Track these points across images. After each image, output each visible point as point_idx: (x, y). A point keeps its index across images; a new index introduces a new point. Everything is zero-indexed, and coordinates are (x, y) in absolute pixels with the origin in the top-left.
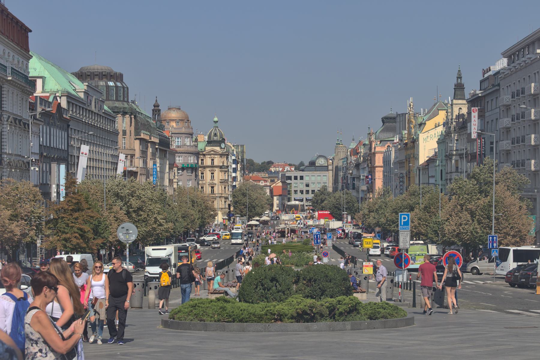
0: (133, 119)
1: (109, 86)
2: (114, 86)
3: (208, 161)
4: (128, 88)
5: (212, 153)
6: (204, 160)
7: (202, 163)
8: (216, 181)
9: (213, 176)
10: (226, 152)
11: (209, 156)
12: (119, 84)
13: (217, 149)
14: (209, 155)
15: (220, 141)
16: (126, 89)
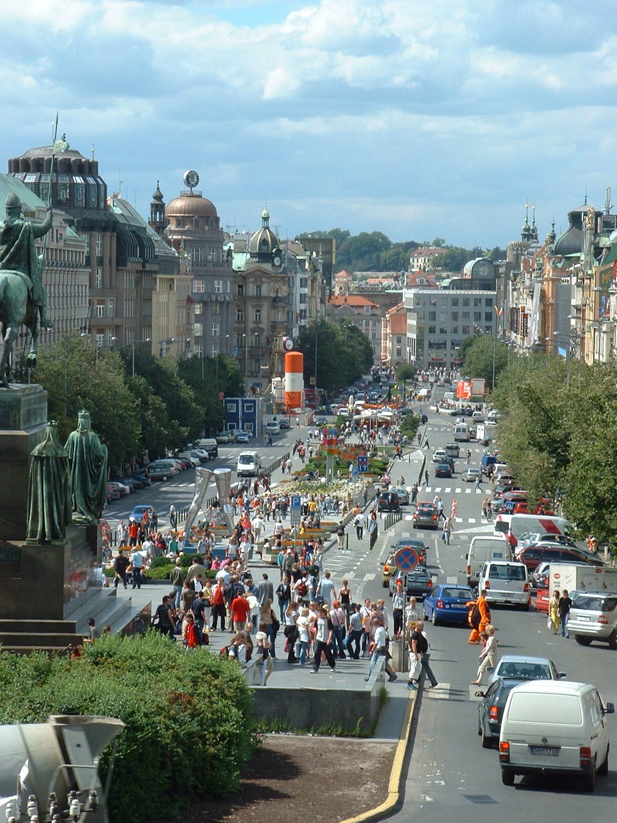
0: (115, 239)
1: (74, 183)
2: (82, 184)
3: (251, 290)
4: (105, 186)
5: (258, 273)
6: (244, 287)
7: (240, 294)
8: (264, 325)
9: (259, 315)
10: (281, 273)
11: (252, 280)
12: (91, 180)
13: (267, 267)
14: (252, 277)
15: (272, 254)
16: (102, 189)
